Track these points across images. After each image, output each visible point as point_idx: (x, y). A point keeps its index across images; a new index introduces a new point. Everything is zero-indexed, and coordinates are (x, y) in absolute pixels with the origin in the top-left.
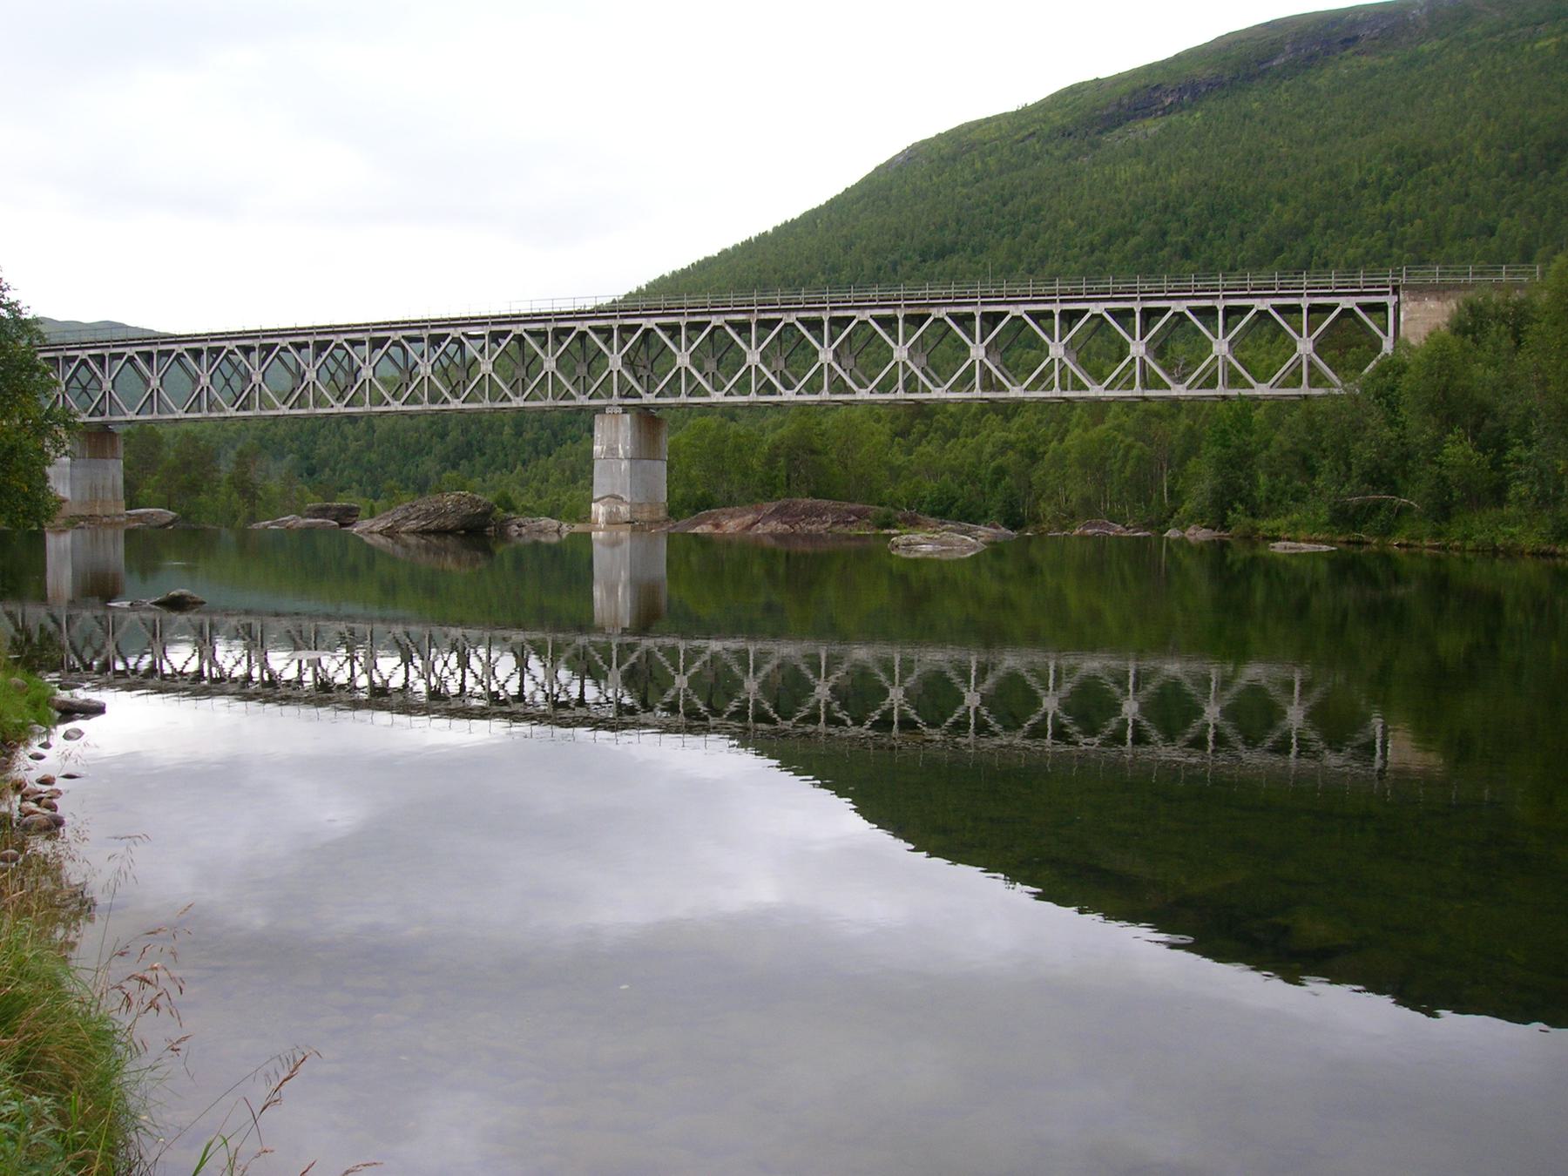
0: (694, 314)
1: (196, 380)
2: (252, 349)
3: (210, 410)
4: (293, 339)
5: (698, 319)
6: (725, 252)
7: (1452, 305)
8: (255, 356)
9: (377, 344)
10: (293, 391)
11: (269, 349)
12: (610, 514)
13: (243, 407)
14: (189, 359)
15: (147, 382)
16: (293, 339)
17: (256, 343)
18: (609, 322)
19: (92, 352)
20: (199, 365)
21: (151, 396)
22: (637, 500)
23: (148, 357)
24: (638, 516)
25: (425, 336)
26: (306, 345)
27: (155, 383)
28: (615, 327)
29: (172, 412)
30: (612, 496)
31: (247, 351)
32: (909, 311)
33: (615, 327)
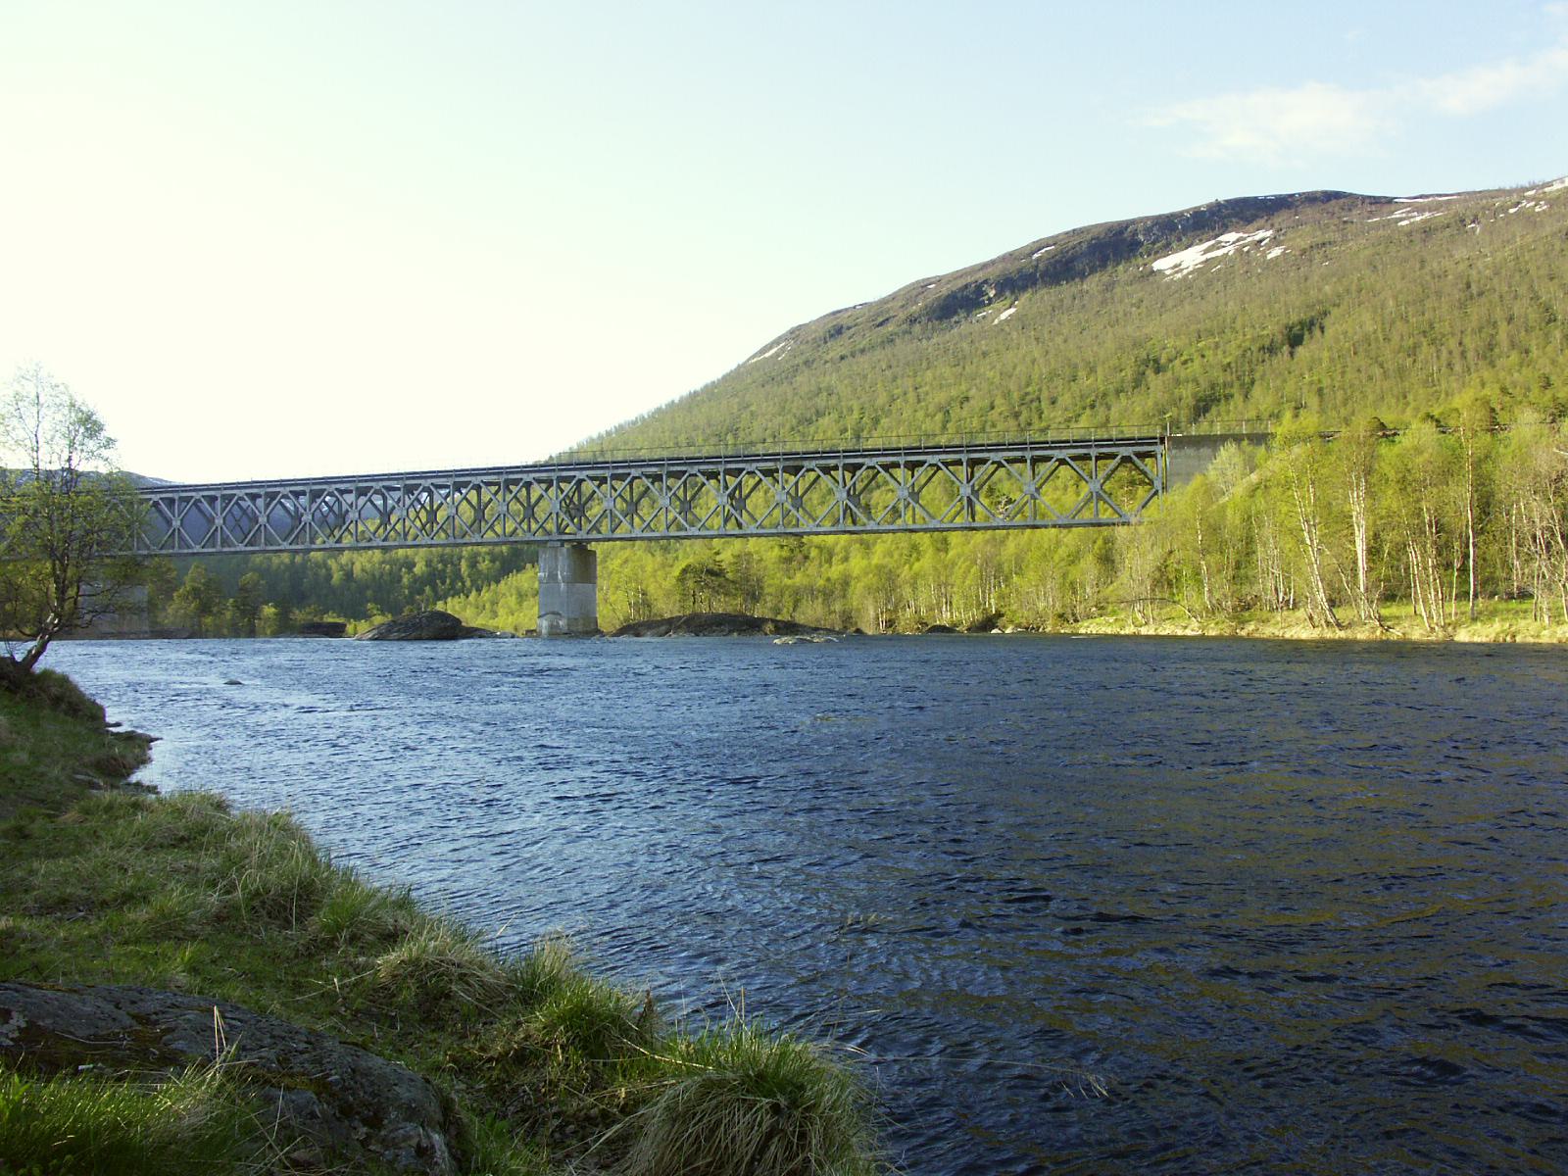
0: (617, 468)
1: (211, 521)
2: (216, 498)
3: (180, 548)
4: (248, 491)
5: (620, 471)
6: (659, 410)
7: (134, 779)
8: (260, 502)
9: (362, 492)
10: (292, 531)
11: (272, 496)
12: (551, 627)
13: (250, 544)
14: (205, 505)
15: (169, 522)
16: (248, 491)
17: (262, 491)
18: (552, 474)
19: (163, 496)
20: (214, 509)
21: (173, 533)
22: (573, 616)
23: (171, 502)
24: (574, 629)
25: (262, 493)
26: (303, 493)
27: (176, 523)
28: (554, 478)
29: (189, 547)
30: (553, 613)
31: (254, 497)
32: (788, 463)
33: (554, 478)
